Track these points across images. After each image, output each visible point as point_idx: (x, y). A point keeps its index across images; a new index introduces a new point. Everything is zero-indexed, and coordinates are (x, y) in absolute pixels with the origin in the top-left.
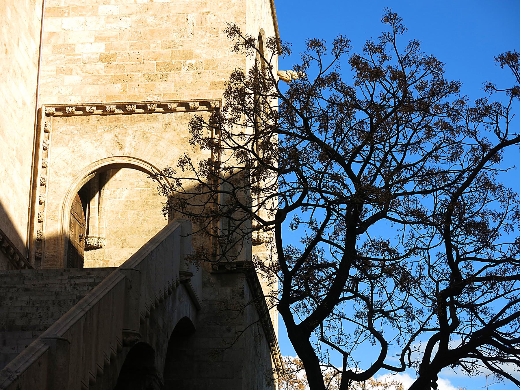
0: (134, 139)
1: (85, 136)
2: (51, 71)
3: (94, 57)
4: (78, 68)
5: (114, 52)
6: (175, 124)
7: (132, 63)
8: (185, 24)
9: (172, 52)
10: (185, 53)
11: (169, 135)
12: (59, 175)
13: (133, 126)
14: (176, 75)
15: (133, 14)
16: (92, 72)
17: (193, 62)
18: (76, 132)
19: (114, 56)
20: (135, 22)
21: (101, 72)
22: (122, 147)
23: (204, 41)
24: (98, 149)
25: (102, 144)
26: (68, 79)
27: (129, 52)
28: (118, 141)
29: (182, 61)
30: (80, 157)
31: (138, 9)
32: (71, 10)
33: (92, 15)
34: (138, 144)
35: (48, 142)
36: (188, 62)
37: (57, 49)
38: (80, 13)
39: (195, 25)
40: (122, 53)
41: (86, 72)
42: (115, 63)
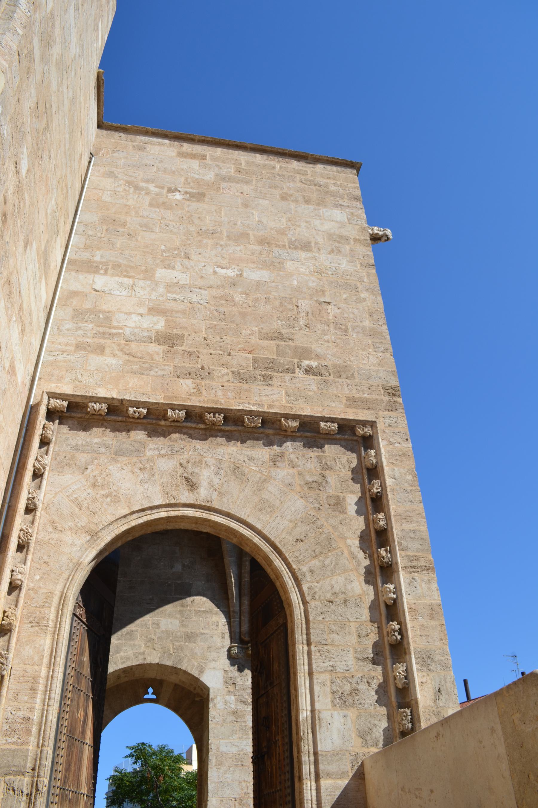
0: (217, 474)
1: (120, 459)
2: (67, 344)
3: (146, 334)
4: (115, 347)
5: (180, 333)
6: (292, 456)
7: (212, 352)
8: (295, 312)
9: (278, 345)
10: (299, 350)
11: (283, 473)
12: (59, 528)
13: (215, 451)
14: (287, 379)
15: (211, 287)
16: (140, 356)
17: (314, 364)
18: (103, 450)
19: (180, 338)
20: (215, 298)
21: (156, 357)
22: (192, 486)
23: (326, 338)
24: (146, 486)
25: (154, 478)
26: (95, 360)
27: (206, 336)
28: (185, 475)
29: (296, 361)
30: (107, 496)
31: (219, 283)
32: (110, 267)
33: (145, 279)
34: (226, 484)
35: (47, 460)
36: (306, 363)
37: (79, 315)
38: (125, 273)
39: (310, 316)
40: (193, 335)
41: (130, 354)
42: (183, 348)
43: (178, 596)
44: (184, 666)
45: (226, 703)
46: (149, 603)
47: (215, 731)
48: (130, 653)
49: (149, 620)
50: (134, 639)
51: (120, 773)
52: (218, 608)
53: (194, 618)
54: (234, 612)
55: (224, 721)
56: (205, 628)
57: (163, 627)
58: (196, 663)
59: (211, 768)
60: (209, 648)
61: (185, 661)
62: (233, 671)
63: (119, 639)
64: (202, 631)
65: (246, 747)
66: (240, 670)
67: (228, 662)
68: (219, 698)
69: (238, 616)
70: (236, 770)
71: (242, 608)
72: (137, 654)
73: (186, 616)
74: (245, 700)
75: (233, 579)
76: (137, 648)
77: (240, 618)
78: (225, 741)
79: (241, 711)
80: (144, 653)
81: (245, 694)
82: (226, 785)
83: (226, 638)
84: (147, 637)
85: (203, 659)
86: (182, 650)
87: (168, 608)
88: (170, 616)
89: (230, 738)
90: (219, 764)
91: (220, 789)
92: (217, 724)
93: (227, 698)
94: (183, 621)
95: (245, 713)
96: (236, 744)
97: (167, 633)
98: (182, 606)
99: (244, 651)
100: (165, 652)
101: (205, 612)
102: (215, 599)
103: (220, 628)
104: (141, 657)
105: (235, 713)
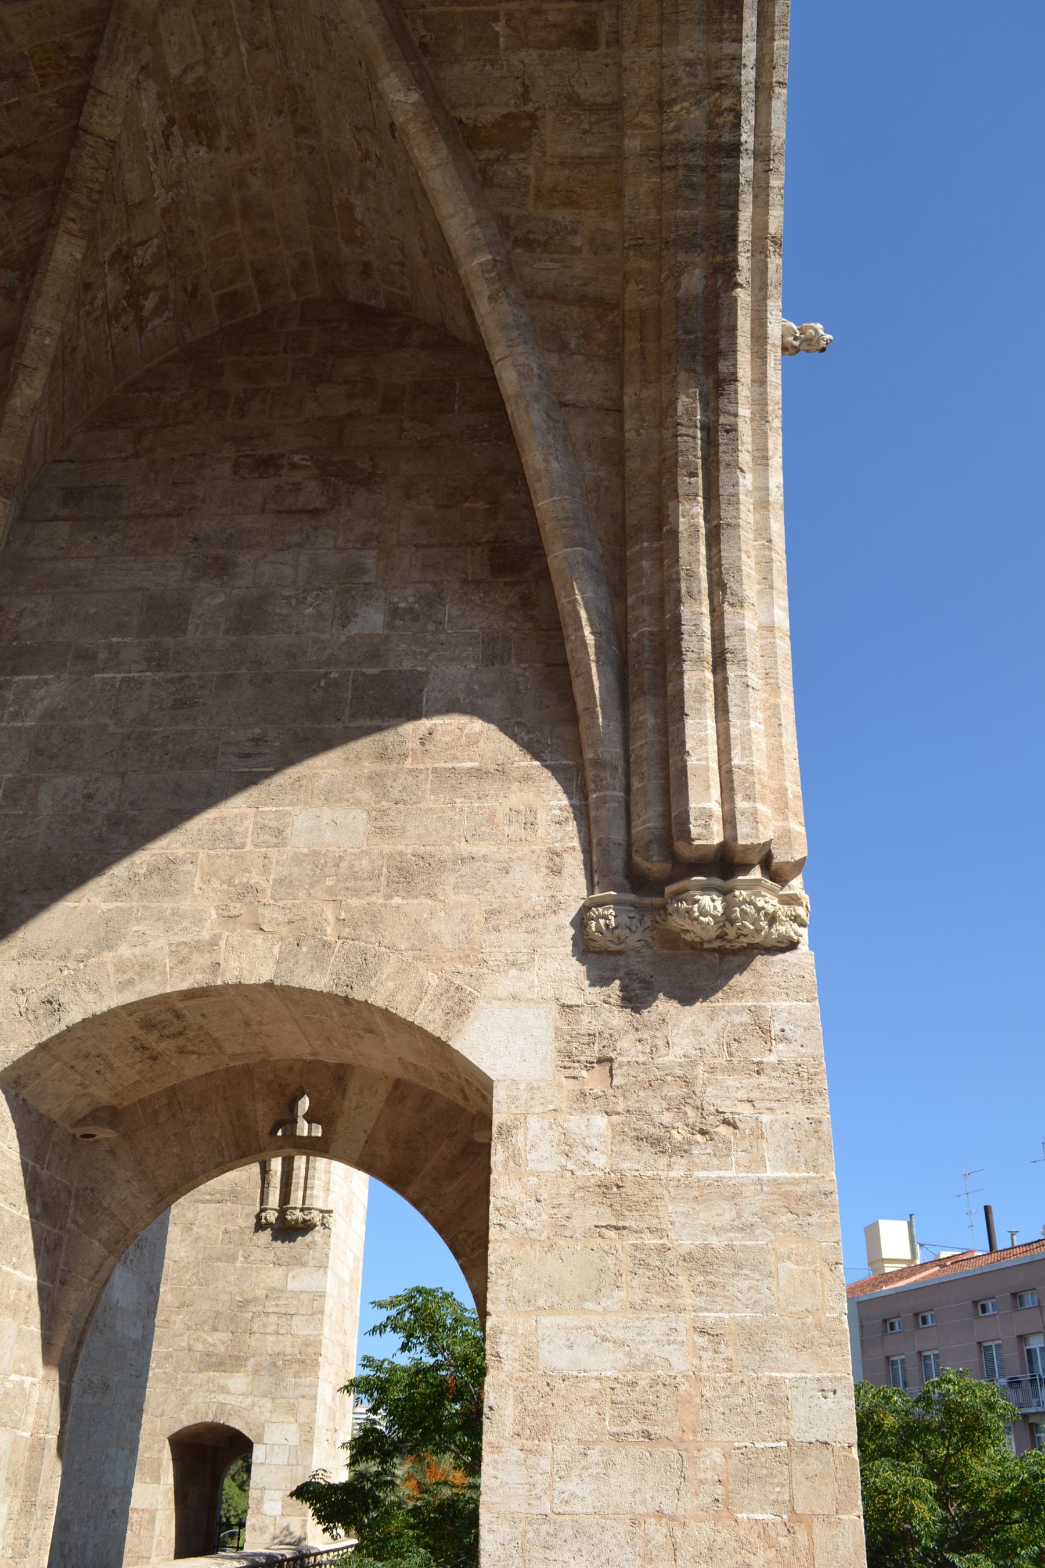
43: (367, 723)
44: (381, 992)
45: (567, 1146)
46: (247, 756)
47: (517, 1272)
48: (159, 944)
49: (243, 817)
50: (177, 892)
51: (379, 1368)
52: (536, 756)
53: (430, 802)
54: (597, 763)
55: (560, 1227)
56: (478, 836)
57: (299, 841)
58: (433, 979)
59: (497, 1449)
60: (491, 913)
61: (389, 969)
62: (603, 1009)
63: (116, 895)
64: (465, 849)
65: (667, 1351)
66: (635, 1000)
67: (576, 970)
68: (535, 1124)
69: (619, 781)
70: (619, 1458)
71: (635, 746)
72: (184, 951)
73: (395, 793)
74: (659, 1132)
75: (587, 631)
76: (185, 924)
77: (628, 789)
78: (561, 1320)
79: (639, 1182)
80: (213, 943)
81: (655, 1106)
82: (569, 1531)
83: (566, 872)
84: (230, 881)
85: (465, 959)
86: (375, 924)
87: (325, 767)
88: (330, 796)
89: (589, 1305)
90: (536, 1430)
91: (537, 1553)
92: (525, 1239)
93: (575, 1123)
94: (384, 812)
95: (657, 1191)
96: (617, 1334)
97: (317, 861)
98: (382, 756)
99: (648, 922)
100: (302, 936)
101: (479, 774)
102: (519, 724)
103: (541, 832)
104: (201, 960)
105: (609, 1189)
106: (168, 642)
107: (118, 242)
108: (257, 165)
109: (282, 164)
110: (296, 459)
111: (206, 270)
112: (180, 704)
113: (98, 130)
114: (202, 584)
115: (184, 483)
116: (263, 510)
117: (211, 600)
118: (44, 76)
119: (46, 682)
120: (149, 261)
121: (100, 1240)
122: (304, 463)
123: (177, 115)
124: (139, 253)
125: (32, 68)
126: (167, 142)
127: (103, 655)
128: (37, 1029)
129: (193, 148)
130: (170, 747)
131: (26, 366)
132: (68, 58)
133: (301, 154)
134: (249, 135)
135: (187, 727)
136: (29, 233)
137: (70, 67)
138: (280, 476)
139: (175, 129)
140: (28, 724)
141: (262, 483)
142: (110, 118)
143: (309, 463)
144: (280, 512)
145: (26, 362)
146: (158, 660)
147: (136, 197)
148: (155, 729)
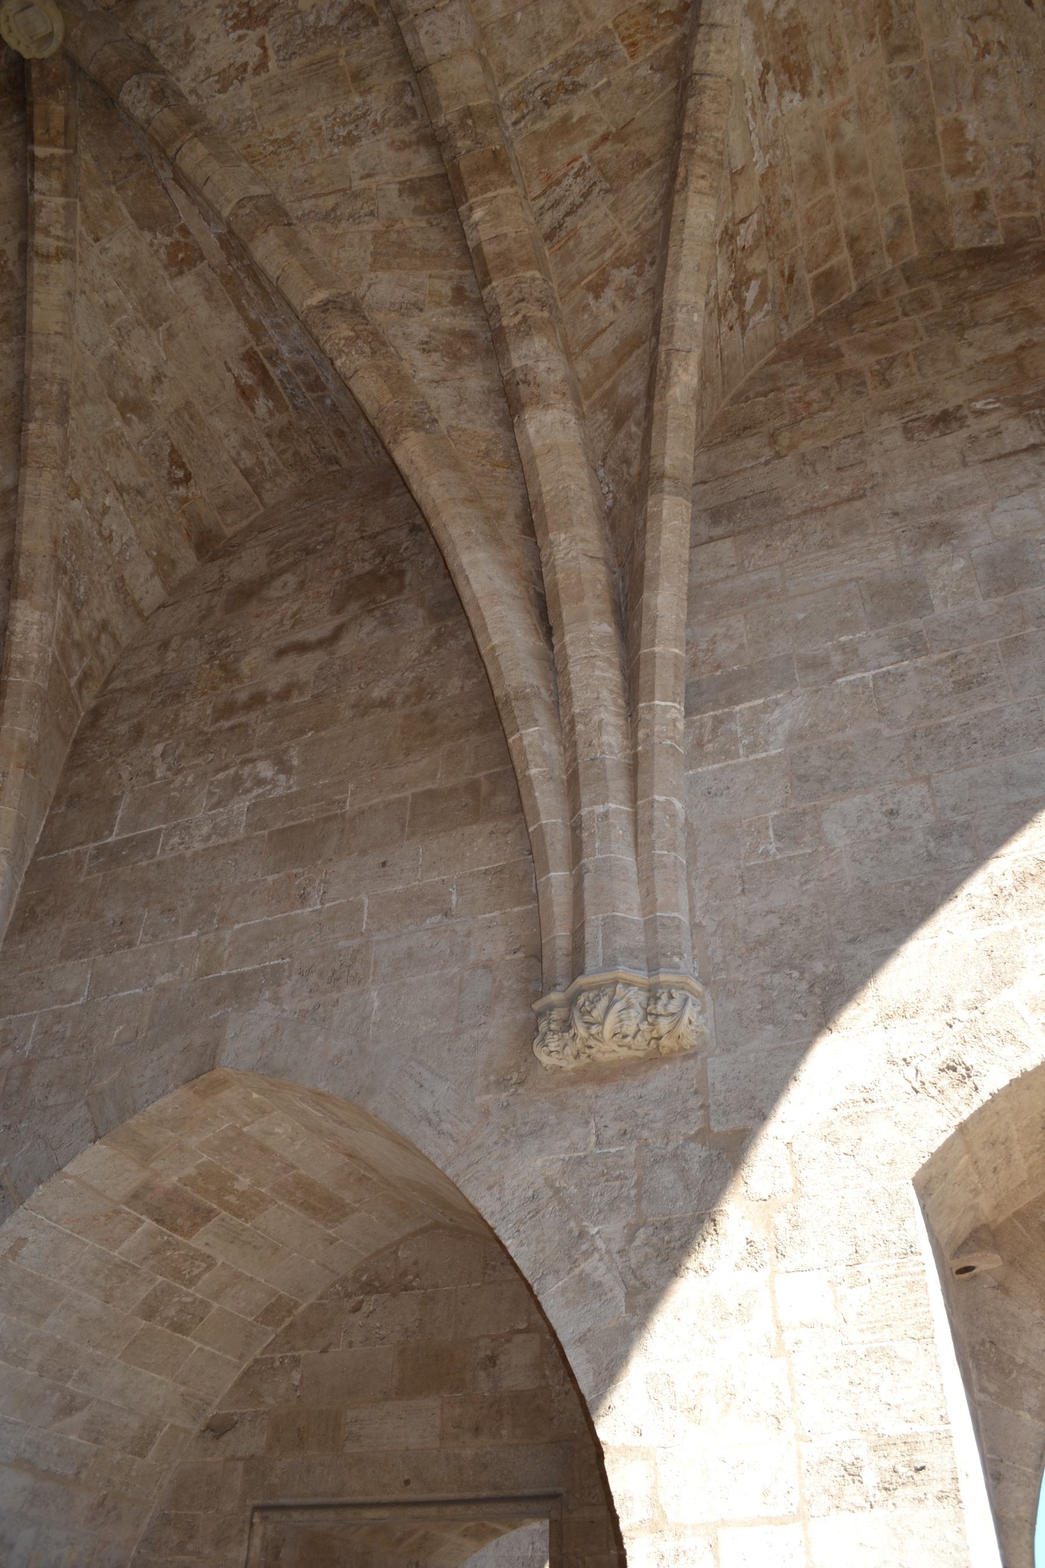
106: (915, 624)
107: (725, 218)
108: (850, 107)
109: (875, 100)
110: (979, 405)
111: (801, 248)
112: (964, 685)
113: (717, 68)
114: (928, 555)
115: (851, 465)
116: (965, 465)
117: (946, 570)
118: (634, 44)
119: (777, 703)
120: (751, 242)
121: (1029, 1410)
122: (991, 406)
123: (771, 59)
124: (742, 231)
125: (618, 41)
126: (763, 93)
127: (837, 658)
128: (948, 1105)
129: (788, 96)
130: (975, 733)
131: (678, 350)
132: (659, 16)
133: (895, 82)
134: (841, 72)
135: (988, 707)
136: (640, 220)
137: (662, 25)
138: (968, 426)
139: (770, 77)
140: (774, 752)
141: (949, 439)
142: (728, 52)
143: (997, 405)
144: (986, 461)
145: (678, 345)
146: (914, 645)
147: (738, 163)
148: (945, 720)
